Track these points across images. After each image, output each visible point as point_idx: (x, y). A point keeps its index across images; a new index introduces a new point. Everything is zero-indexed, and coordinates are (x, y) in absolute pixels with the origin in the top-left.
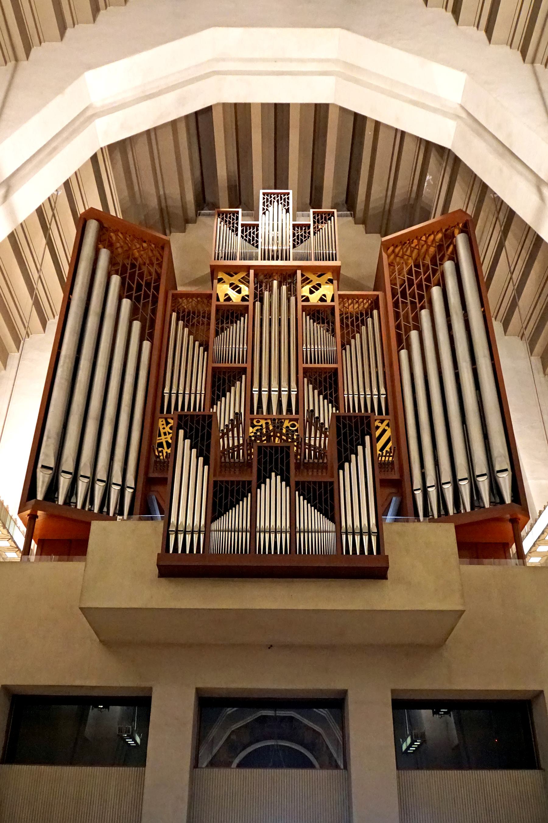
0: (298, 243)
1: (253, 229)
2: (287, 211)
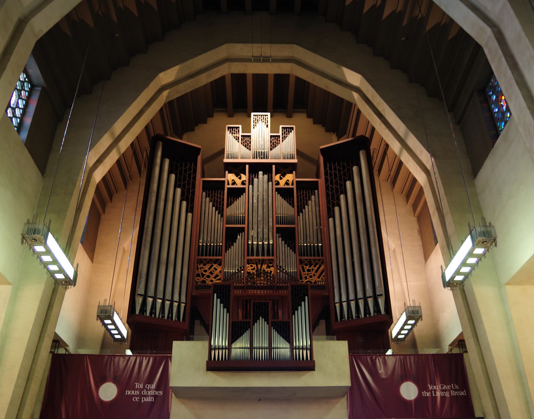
0: (273, 147)
1: (248, 138)
2: (267, 126)
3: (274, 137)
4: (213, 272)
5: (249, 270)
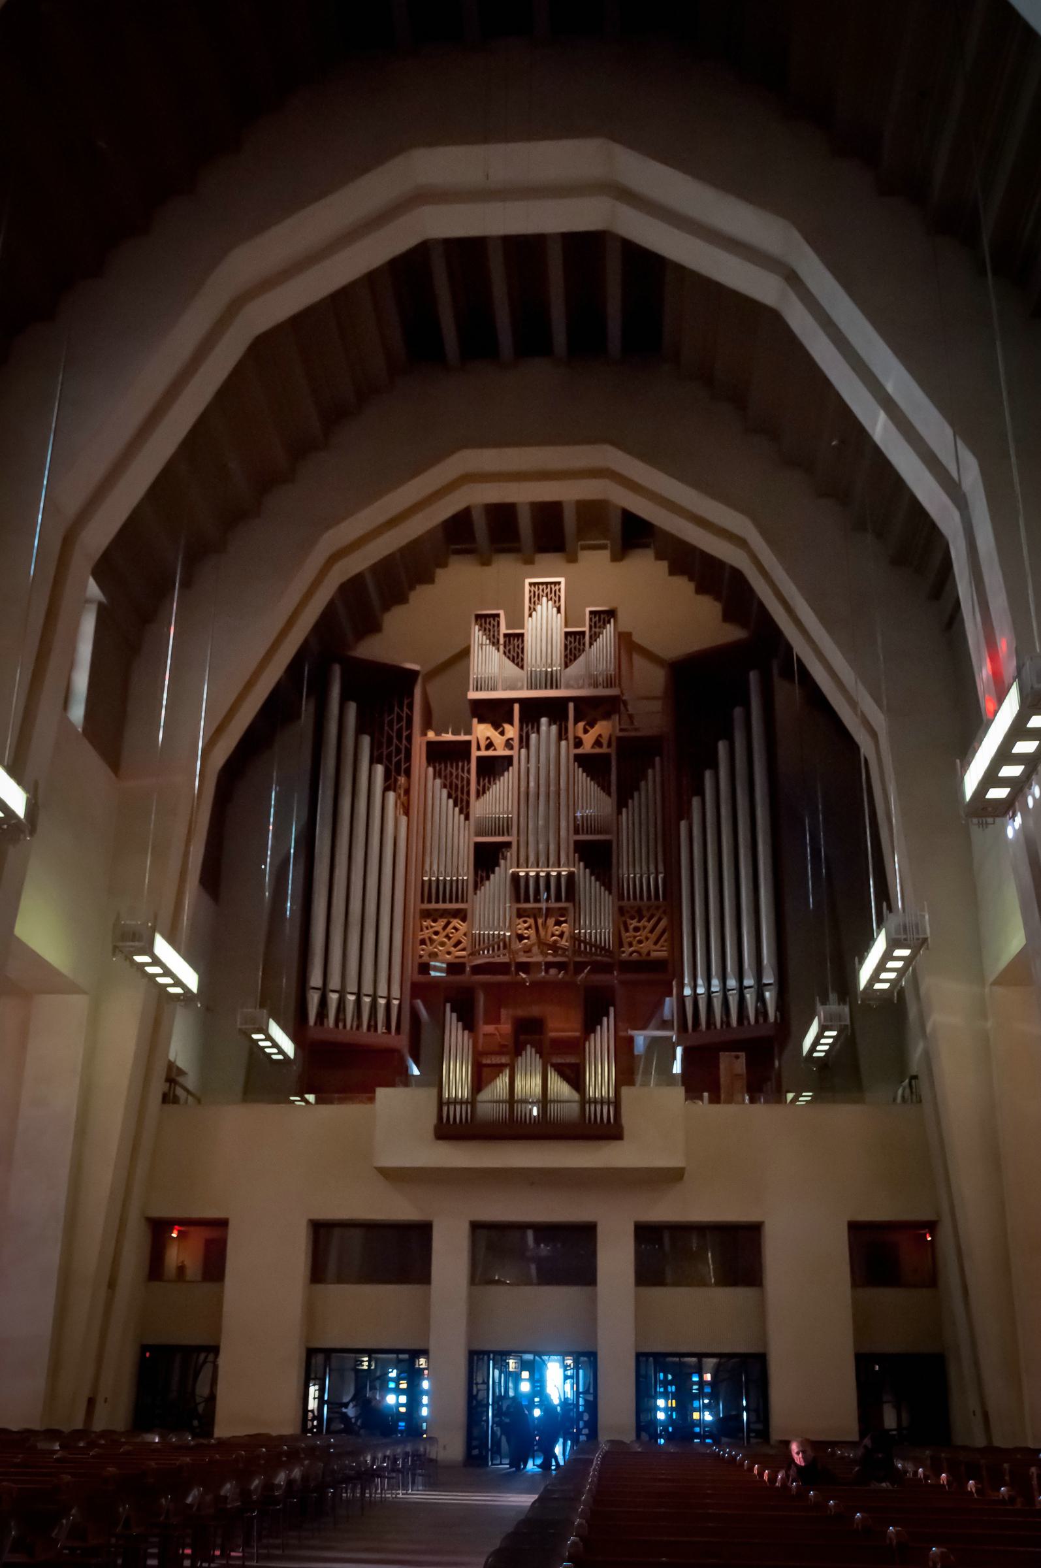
1: (518, 640)
3: (573, 637)
4: (451, 935)
5: (520, 929)
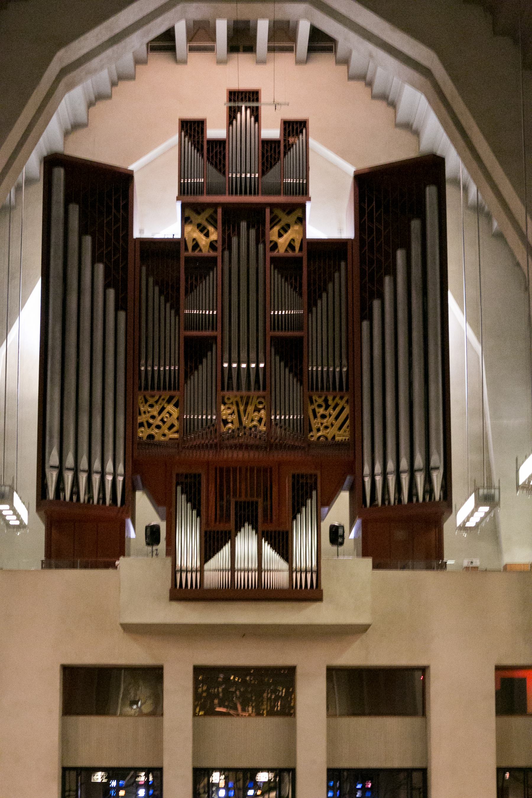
0: (267, 168)
4: (165, 420)
